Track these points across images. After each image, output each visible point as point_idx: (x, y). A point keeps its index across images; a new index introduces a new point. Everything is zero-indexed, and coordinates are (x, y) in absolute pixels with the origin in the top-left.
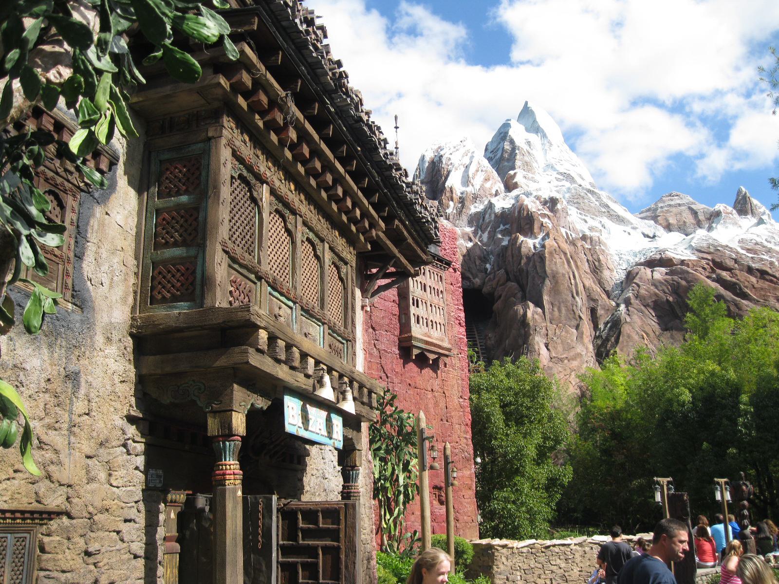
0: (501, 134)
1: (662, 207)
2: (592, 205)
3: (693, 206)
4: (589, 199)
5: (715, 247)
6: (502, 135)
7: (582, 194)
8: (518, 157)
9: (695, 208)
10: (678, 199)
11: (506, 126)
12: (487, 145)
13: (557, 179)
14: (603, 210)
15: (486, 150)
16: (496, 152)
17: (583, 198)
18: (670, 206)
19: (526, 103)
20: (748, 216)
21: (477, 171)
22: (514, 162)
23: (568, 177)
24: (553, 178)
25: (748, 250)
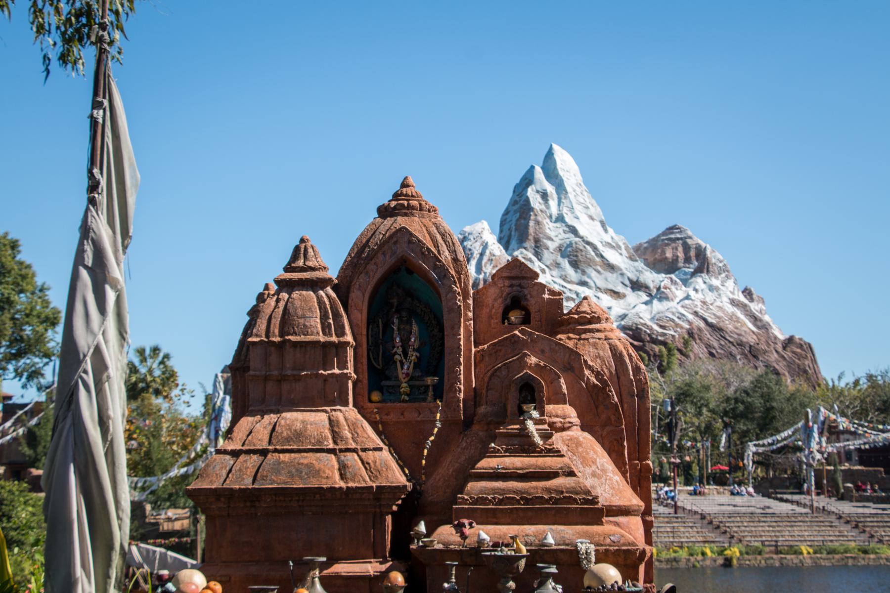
0: (526, 179)
1: (663, 240)
2: (588, 256)
3: (689, 241)
4: (587, 251)
5: (636, 324)
6: (527, 181)
7: (581, 248)
8: (532, 218)
9: (690, 243)
10: (678, 232)
11: (532, 168)
12: (515, 187)
13: (565, 232)
14: (597, 259)
15: (514, 191)
16: (521, 197)
17: (581, 250)
18: (670, 239)
19: (551, 146)
20: (703, 275)
21: (489, 260)
22: (528, 222)
23: (574, 231)
24: (561, 231)
25: (661, 327)
